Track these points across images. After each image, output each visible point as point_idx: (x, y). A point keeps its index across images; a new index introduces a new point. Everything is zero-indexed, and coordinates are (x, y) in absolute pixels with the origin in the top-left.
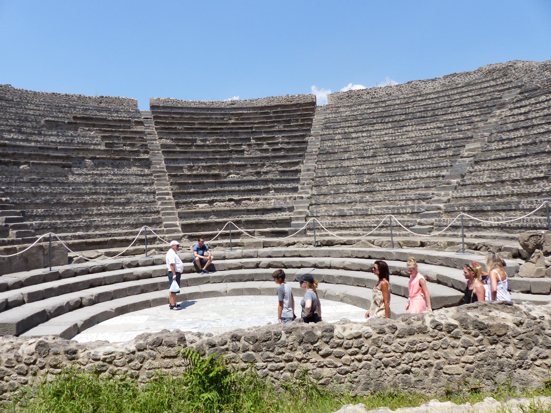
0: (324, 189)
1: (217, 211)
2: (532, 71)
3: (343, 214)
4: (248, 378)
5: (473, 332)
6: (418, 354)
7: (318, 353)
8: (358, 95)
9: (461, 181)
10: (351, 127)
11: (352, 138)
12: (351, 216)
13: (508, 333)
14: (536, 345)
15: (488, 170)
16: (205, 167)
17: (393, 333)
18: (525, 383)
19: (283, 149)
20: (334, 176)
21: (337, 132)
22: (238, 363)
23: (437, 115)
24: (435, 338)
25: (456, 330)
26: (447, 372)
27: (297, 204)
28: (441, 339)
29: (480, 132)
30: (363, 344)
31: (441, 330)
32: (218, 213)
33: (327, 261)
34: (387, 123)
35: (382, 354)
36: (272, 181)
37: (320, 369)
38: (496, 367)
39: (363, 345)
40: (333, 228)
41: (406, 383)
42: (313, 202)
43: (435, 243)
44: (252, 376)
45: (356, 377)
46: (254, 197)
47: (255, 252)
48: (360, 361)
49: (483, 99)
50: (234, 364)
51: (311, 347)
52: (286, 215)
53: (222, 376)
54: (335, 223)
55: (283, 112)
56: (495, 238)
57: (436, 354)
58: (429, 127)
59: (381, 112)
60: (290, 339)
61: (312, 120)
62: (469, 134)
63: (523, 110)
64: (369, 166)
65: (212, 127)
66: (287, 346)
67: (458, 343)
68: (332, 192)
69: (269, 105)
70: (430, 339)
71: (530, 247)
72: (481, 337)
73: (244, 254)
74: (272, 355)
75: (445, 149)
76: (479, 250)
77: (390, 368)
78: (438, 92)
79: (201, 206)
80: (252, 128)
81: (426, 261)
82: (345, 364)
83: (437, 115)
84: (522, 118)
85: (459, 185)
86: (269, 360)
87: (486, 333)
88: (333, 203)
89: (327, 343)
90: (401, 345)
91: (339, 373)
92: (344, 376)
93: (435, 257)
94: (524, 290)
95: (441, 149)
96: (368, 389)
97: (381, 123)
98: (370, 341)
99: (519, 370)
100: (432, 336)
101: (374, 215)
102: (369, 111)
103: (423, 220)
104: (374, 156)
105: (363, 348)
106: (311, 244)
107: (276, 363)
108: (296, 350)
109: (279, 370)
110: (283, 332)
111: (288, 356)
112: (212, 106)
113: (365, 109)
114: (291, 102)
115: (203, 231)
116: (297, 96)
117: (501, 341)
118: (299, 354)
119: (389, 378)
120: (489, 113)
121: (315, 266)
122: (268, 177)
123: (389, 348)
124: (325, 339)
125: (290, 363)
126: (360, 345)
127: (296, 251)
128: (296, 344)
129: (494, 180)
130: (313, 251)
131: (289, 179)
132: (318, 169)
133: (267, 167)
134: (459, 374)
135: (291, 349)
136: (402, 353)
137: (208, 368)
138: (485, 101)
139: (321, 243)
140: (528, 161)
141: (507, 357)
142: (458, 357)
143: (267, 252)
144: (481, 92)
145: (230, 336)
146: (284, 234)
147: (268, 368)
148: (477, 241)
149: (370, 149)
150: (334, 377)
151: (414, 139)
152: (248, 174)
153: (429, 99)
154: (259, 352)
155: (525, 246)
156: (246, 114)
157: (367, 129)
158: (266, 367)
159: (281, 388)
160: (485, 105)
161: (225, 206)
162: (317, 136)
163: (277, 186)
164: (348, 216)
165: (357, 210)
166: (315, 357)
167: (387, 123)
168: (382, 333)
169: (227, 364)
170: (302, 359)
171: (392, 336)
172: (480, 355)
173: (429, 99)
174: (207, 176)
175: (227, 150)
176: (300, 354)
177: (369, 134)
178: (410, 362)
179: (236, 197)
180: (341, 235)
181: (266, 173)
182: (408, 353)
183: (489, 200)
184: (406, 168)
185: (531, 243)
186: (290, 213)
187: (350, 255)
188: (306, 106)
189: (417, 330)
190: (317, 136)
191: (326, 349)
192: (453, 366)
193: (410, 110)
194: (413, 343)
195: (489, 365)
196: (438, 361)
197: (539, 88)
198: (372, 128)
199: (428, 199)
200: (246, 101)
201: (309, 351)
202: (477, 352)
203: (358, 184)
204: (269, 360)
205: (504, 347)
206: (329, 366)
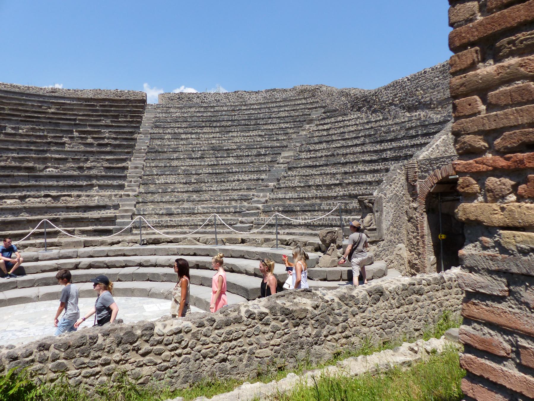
0: (152, 188)
1: (30, 208)
2: (332, 95)
3: (170, 213)
4: (58, 389)
5: (281, 318)
6: (234, 343)
7: (137, 352)
8: (189, 98)
9: (277, 184)
10: (181, 128)
11: (182, 139)
12: (178, 214)
13: (308, 316)
14: (328, 324)
15: (298, 176)
16: (16, 158)
17: (212, 326)
18: (320, 356)
19: (110, 144)
20: (162, 175)
21: (167, 132)
22: (46, 374)
23: (259, 124)
24: (249, 327)
25: (267, 317)
26: (259, 356)
27: (123, 201)
28: (254, 326)
29: (293, 143)
30: (183, 339)
31: (254, 319)
32: (31, 210)
33: (153, 259)
34: (215, 127)
35: (201, 346)
36: (96, 177)
37: (139, 369)
38: (298, 346)
39: (183, 340)
40: (160, 226)
41: (223, 371)
42: (140, 200)
43: (254, 240)
44: (62, 386)
45: (176, 372)
46: (75, 193)
47: (74, 252)
48: (179, 355)
49: (296, 114)
50: (41, 377)
51: (130, 347)
52: (110, 213)
53: (25, 392)
54: (162, 221)
55: (111, 106)
56: (302, 234)
57: (249, 341)
58: (252, 135)
59: (210, 116)
60: (108, 341)
61: (141, 117)
62: (285, 143)
63: (326, 127)
64: (197, 167)
65: (26, 114)
66: (104, 349)
67: (268, 328)
68: (160, 191)
69: (96, 97)
70: (244, 328)
71: (327, 242)
72: (286, 321)
73: (61, 255)
74: (86, 360)
75: (265, 155)
76: (289, 245)
77: (209, 359)
78: (260, 104)
79: (9, 201)
80: (75, 120)
81: (245, 257)
82: (164, 361)
83: (259, 124)
84: (325, 133)
85: (275, 187)
86: (83, 366)
87: (291, 317)
88: (161, 202)
89: (147, 341)
90: (219, 336)
91: (158, 370)
92: (164, 372)
93: (253, 252)
94: (322, 278)
95: (261, 155)
96: (187, 382)
97: (210, 127)
98: (190, 335)
99: (315, 347)
100: (246, 325)
101: (201, 213)
102: (198, 114)
103: (244, 219)
104: (202, 158)
105: (183, 343)
106: (136, 243)
107: (92, 368)
108: (114, 352)
109: (94, 375)
110: (99, 335)
111: (105, 360)
112: (28, 92)
113: (195, 112)
114: (120, 97)
115: (11, 230)
116: (126, 91)
117: (302, 323)
118: (117, 356)
119: (207, 368)
120: (301, 127)
121: (140, 265)
122: (91, 173)
123: (208, 340)
124: (144, 338)
125: (107, 367)
126: (180, 340)
127: (120, 250)
128: (114, 346)
129: (302, 185)
130: (139, 249)
131: (116, 175)
132: (146, 167)
133: (91, 162)
134: (268, 357)
135: (108, 352)
136: (220, 343)
137: (8, 385)
138: (298, 116)
139: (147, 241)
140: (329, 170)
141: (307, 337)
142: (268, 341)
143: (88, 252)
144: (295, 108)
145: (37, 345)
146: (108, 232)
147: (82, 374)
148: (288, 238)
149: (198, 151)
150: (153, 375)
151: (238, 144)
152: (69, 168)
153: (253, 109)
154: (73, 358)
155: (323, 241)
156: (69, 104)
157: (196, 131)
158: (80, 374)
159: (96, 395)
160: (298, 120)
161: (40, 203)
162: (146, 134)
163: (102, 182)
164: (176, 214)
165: (184, 209)
166: (134, 357)
167: (215, 127)
168: (201, 327)
169: (32, 377)
170: (120, 360)
171: (211, 328)
172: (286, 337)
173: (253, 109)
174: (19, 169)
175: (45, 141)
176: (118, 356)
177: (197, 137)
178: (226, 351)
179: (54, 193)
180: (168, 233)
181: (90, 168)
182: (225, 343)
183: (299, 201)
184: (231, 171)
185: (328, 239)
186: (115, 211)
187: (176, 252)
188: (136, 103)
189: (234, 321)
190: (146, 134)
191: (146, 347)
192: (264, 350)
193: (236, 118)
194: (229, 333)
195: (292, 345)
196: (251, 347)
197: (338, 110)
198: (201, 131)
199: (249, 199)
200: (69, 90)
201: (128, 351)
202: (283, 335)
203: (186, 183)
204: (83, 366)
205: (304, 328)
206: (148, 364)
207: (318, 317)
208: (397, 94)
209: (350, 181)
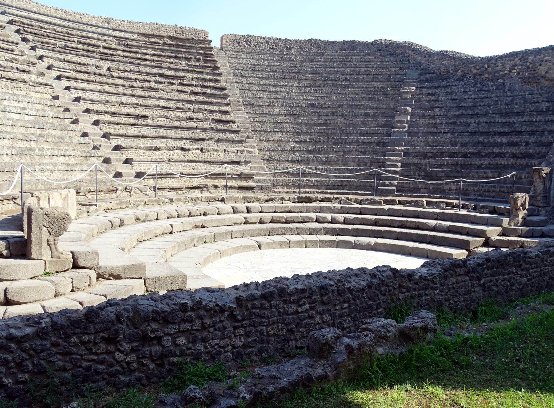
129: (435, 152)
191: (524, 266)
208: (516, 65)
209: (490, 151)
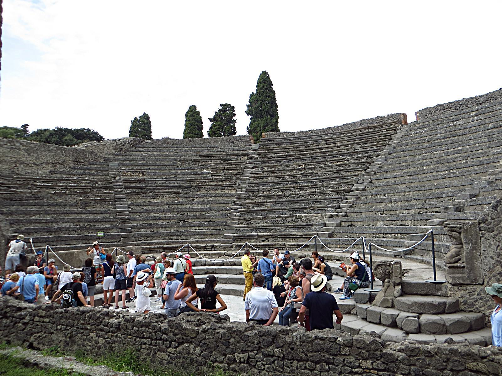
14: (214, 350)
134: (166, 360)
141: (197, 355)
195: (183, 358)
207: (207, 342)
